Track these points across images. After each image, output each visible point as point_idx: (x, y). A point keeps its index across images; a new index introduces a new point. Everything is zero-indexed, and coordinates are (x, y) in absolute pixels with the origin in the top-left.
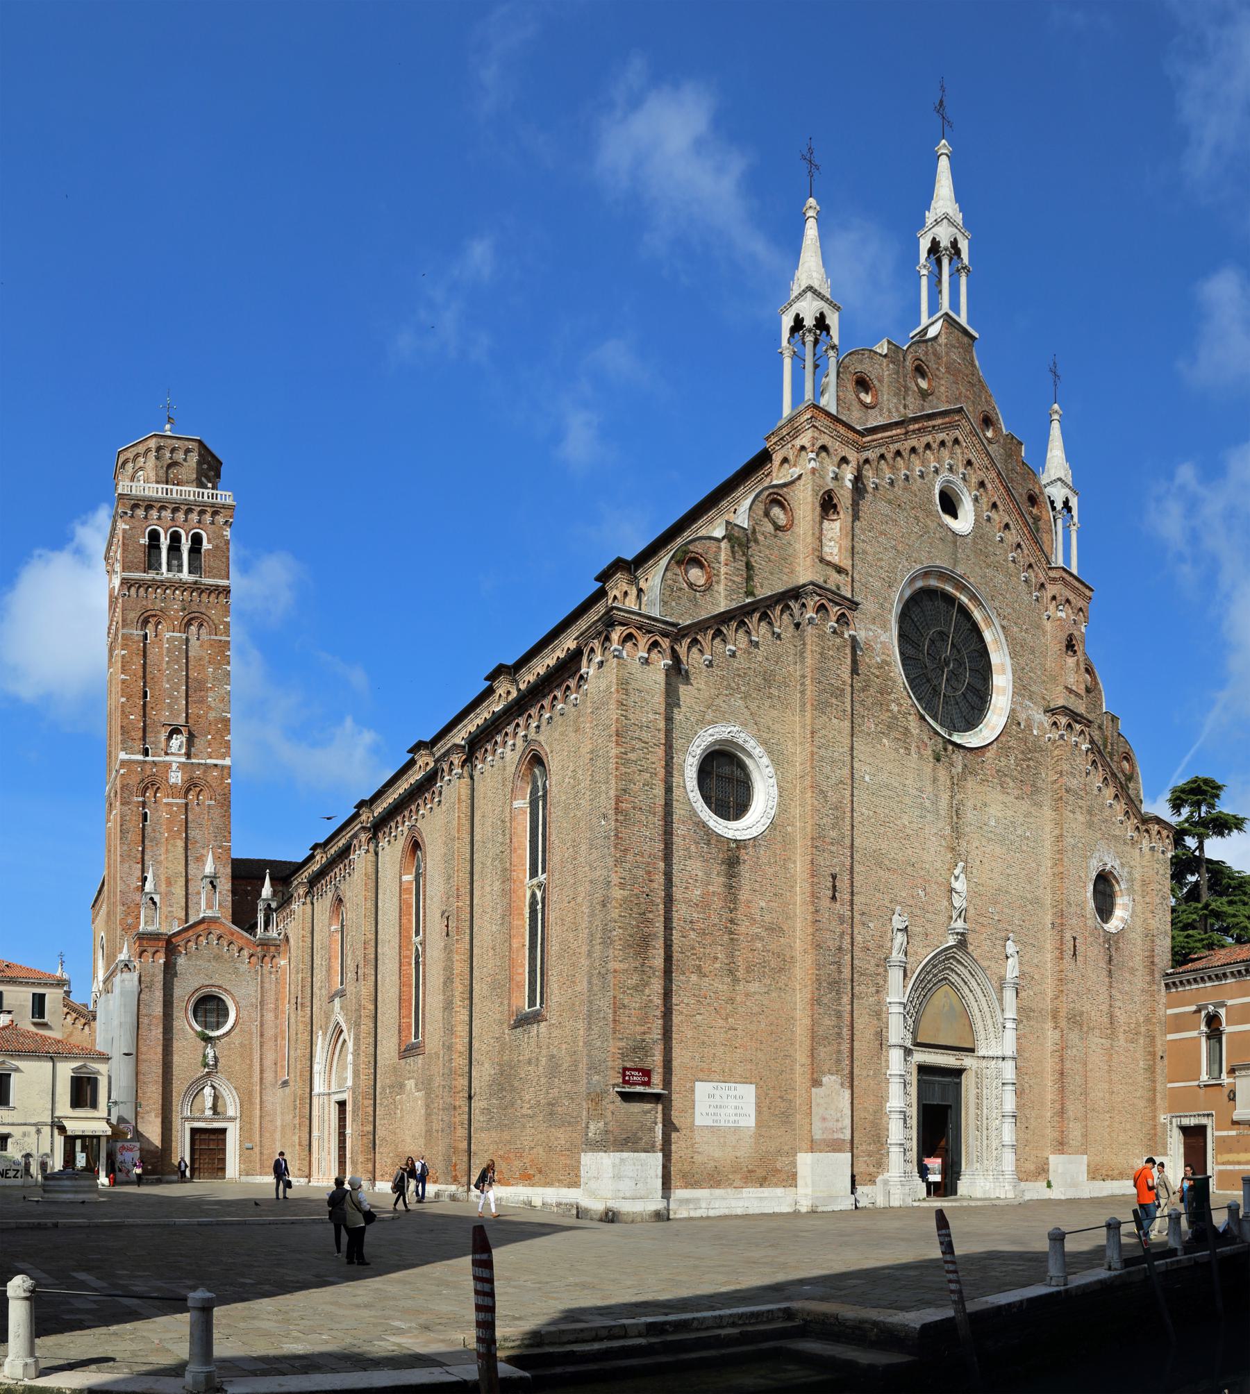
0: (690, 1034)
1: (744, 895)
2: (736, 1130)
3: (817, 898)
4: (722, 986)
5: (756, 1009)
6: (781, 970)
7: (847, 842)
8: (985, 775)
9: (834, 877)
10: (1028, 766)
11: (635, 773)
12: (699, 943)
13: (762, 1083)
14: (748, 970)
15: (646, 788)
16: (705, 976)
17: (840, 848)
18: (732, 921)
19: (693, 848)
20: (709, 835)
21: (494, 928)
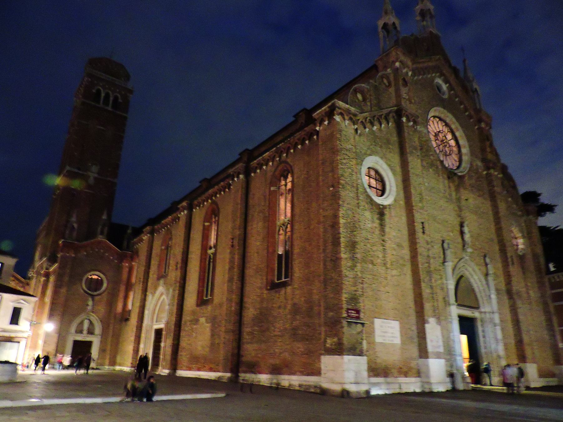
0: (370, 293)
1: (387, 229)
2: (393, 345)
18: (383, 241)
20: (372, 202)
21: (258, 244)
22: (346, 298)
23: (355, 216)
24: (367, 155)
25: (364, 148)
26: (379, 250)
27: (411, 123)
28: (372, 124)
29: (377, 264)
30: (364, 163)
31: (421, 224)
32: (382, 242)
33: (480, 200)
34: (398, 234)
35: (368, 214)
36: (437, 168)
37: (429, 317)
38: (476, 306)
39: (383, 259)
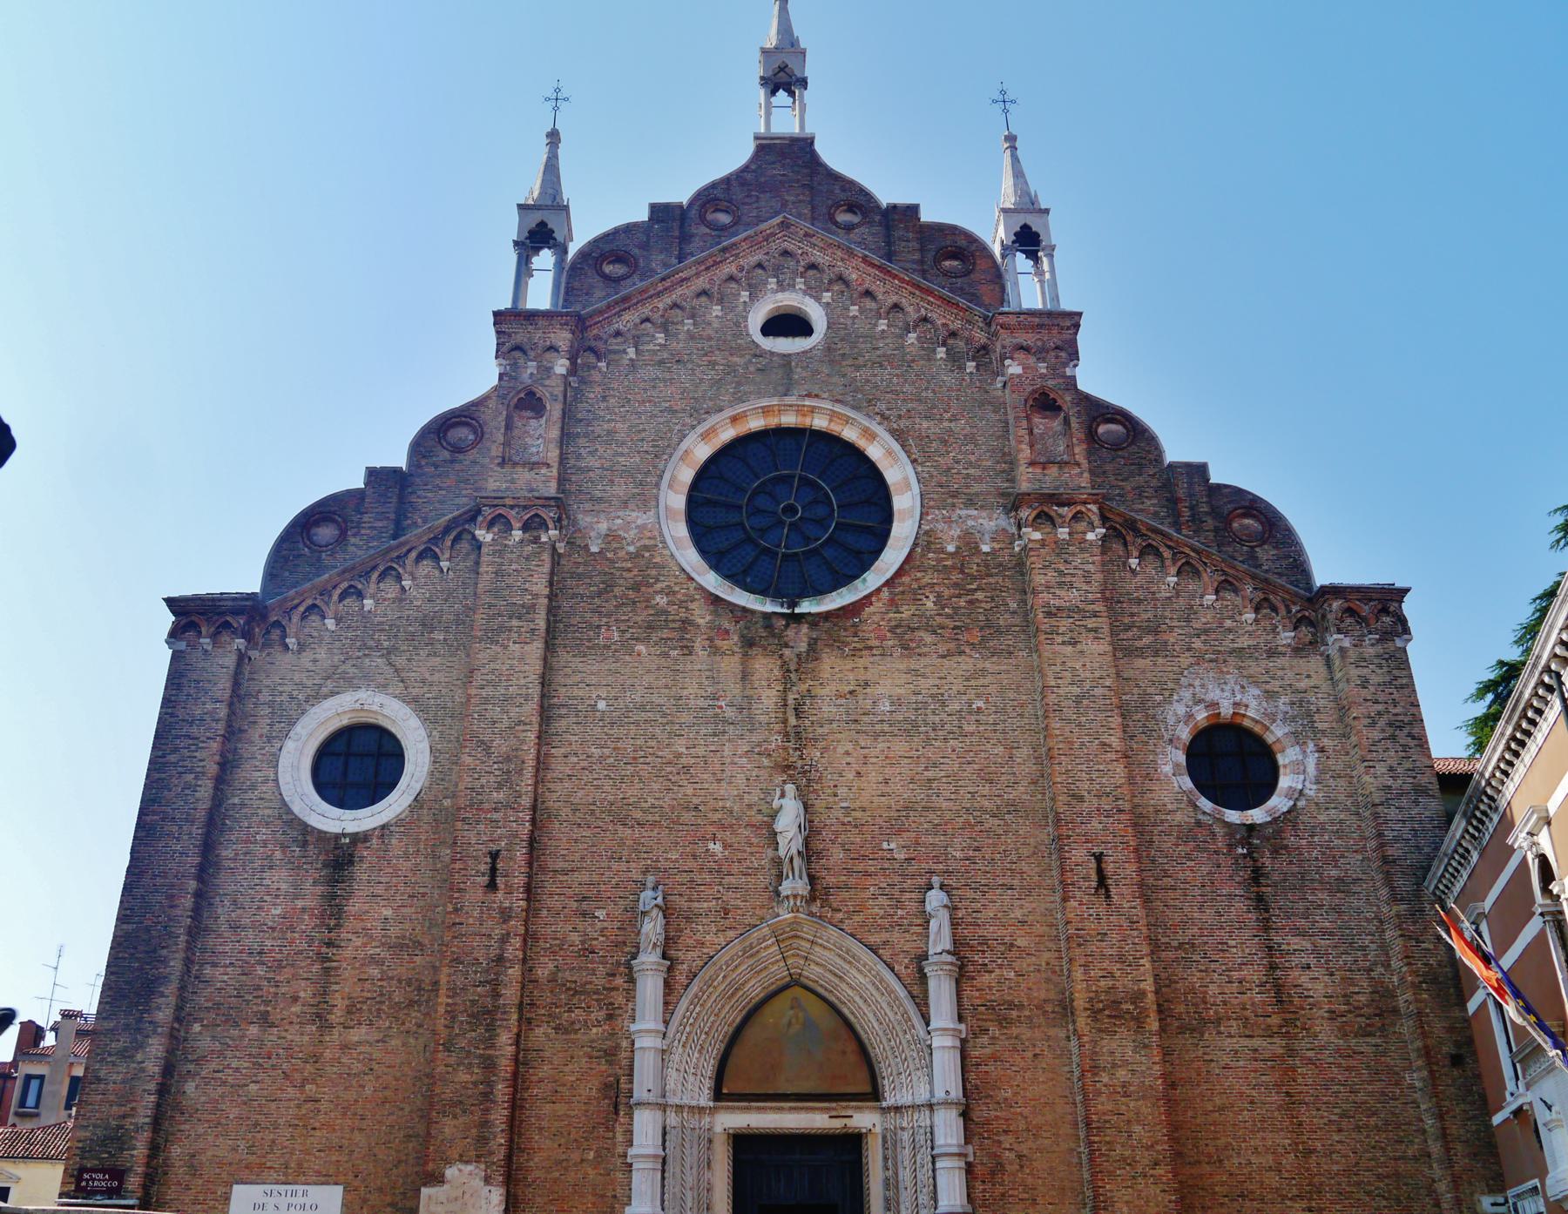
1: (354, 906)
3: (460, 890)
4: (301, 1037)
5: (357, 1067)
6: (411, 1004)
7: (526, 801)
8: (863, 640)
9: (494, 856)
10: (970, 602)
11: (171, 776)
12: (269, 980)
13: (356, 1183)
14: (349, 1011)
15: (187, 792)
16: (273, 1025)
17: (510, 812)
18: (330, 944)
19: (278, 854)
20: (306, 834)
22: (79, 1141)
23: (177, 902)
24: (317, 697)
25: (309, 683)
26: (305, 976)
27: (517, 534)
28: (360, 595)
29: (282, 1019)
30: (298, 728)
31: (489, 860)
32: (324, 950)
33: (966, 663)
34: (405, 910)
35: (279, 879)
36: (686, 623)
37: (449, 1162)
38: (868, 1089)
39: (312, 1001)
